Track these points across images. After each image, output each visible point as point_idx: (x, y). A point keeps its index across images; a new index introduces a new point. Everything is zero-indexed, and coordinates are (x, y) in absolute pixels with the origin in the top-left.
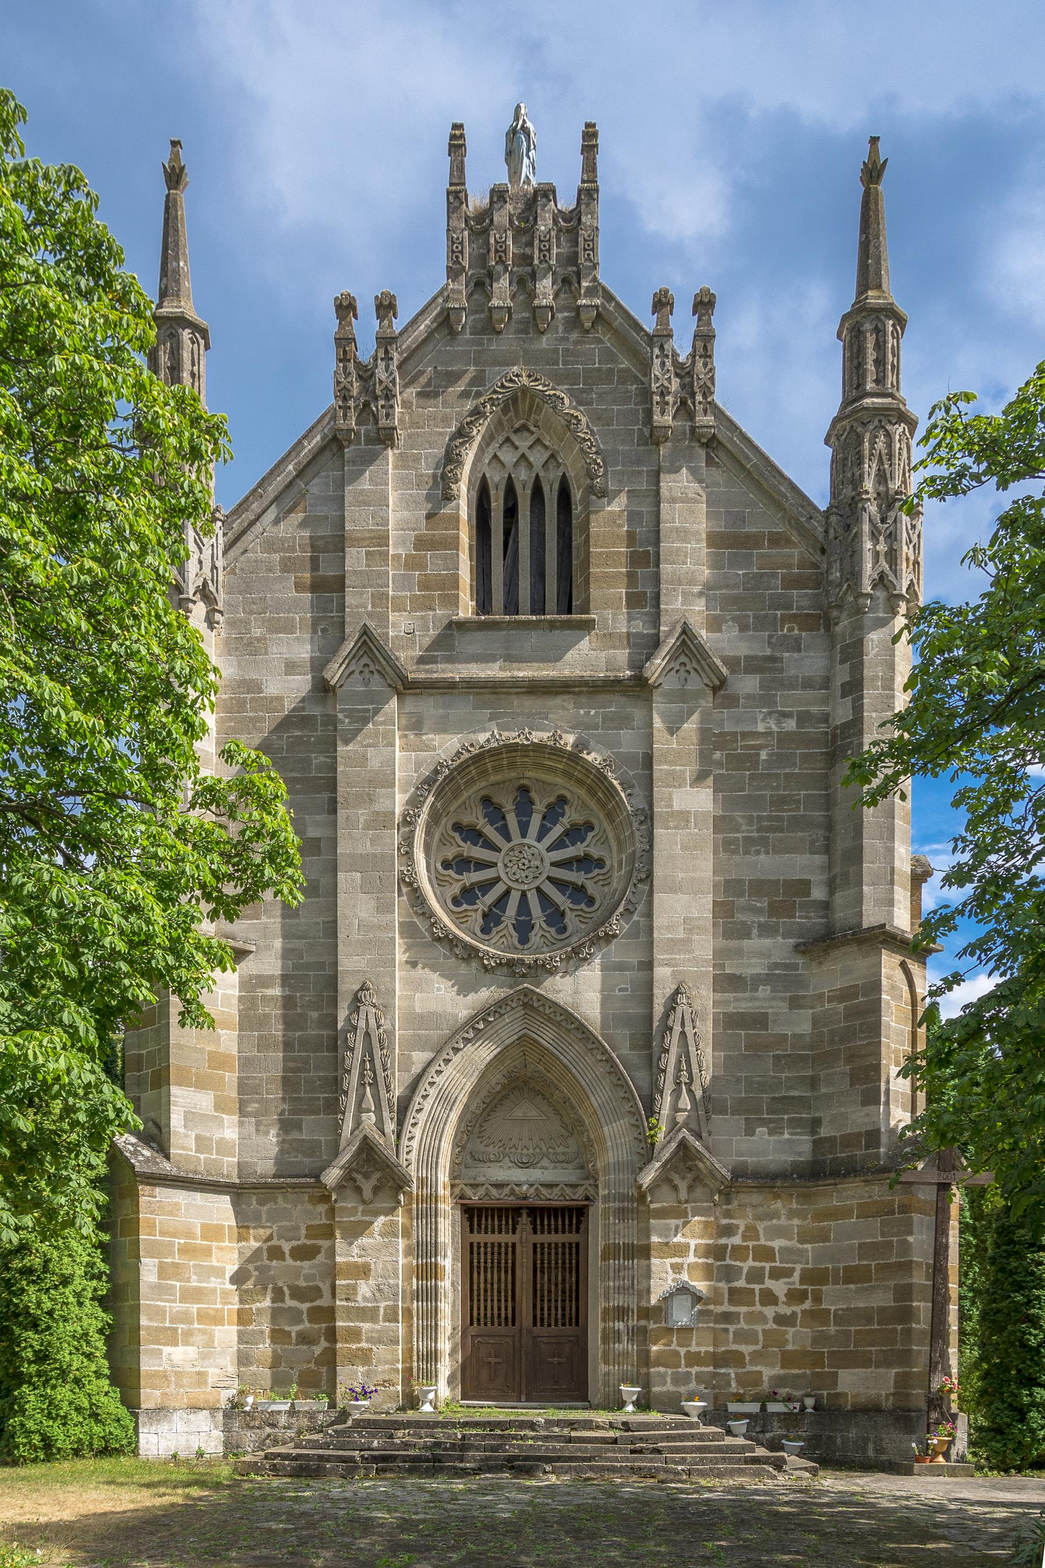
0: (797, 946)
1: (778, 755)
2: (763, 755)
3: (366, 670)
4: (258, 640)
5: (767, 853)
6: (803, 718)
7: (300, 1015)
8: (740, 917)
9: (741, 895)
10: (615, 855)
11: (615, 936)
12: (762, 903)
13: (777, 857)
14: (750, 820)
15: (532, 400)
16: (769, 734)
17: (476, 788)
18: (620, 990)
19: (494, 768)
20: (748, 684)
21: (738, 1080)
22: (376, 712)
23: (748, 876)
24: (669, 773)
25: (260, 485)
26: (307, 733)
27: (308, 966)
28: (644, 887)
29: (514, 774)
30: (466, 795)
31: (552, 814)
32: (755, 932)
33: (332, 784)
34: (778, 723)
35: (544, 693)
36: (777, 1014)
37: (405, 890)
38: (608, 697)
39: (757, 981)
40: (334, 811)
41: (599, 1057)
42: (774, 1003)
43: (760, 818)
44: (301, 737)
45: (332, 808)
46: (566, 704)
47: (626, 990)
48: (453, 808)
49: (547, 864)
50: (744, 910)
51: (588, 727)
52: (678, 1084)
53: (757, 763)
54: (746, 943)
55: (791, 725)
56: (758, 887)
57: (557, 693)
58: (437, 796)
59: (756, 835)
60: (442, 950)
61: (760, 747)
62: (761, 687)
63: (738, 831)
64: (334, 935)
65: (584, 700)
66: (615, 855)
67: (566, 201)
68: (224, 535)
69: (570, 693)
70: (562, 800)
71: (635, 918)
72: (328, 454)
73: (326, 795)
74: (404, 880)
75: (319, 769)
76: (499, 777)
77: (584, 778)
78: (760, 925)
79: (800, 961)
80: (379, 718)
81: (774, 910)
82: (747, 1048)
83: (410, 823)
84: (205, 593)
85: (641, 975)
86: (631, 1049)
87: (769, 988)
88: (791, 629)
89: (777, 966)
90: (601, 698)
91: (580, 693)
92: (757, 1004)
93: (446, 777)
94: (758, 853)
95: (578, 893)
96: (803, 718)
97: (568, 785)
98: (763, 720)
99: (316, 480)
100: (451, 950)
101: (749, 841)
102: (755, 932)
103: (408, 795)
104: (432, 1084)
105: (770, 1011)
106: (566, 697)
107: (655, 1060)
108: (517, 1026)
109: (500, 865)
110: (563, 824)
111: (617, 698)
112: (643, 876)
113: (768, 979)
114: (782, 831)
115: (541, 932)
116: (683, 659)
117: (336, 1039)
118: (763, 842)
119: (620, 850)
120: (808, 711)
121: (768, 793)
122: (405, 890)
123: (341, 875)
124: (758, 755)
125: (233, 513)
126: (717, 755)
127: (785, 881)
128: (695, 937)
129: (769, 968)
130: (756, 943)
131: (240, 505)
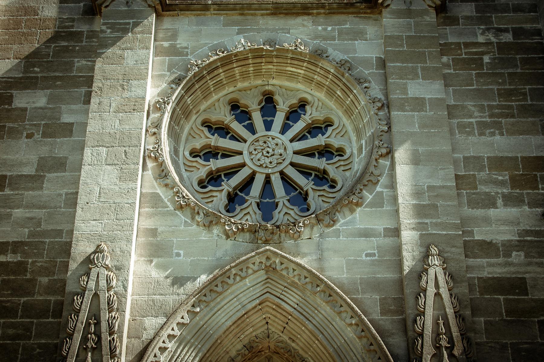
1: (501, 59)
2: (486, 59)
5: (502, 134)
7: (28, 281)
8: (483, 188)
9: (482, 169)
10: (354, 144)
11: (358, 205)
12: (505, 176)
13: (512, 138)
14: (482, 108)
16: (488, 44)
17: (225, 92)
18: (367, 255)
19: (242, 74)
21: (504, 347)
23: (486, 153)
24: (401, 68)
26: (72, 44)
27: (45, 234)
28: (385, 163)
29: (259, 82)
30: (215, 97)
31: (293, 115)
33: (89, 81)
34: (496, 36)
35: (287, 14)
36: (534, 279)
37: (150, 164)
38: (342, 17)
39: (508, 248)
40: (87, 101)
41: (348, 321)
42: (529, 268)
43: (490, 107)
44: (67, 47)
46: (305, 23)
47: (374, 255)
48: (203, 107)
49: (290, 151)
50: (485, 182)
51: (325, 39)
52: (438, 348)
53: (482, 65)
54: (492, 212)
55: (508, 37)
56: (498, 163)
57: (298, 14)
58: (188, 89)
59: (488, 120)
60: (182, 217)
61: (483, 53)
62: (477, 12)
63: (471, 117)
65: (321, 19)
66: (354, 144)
69: (309, 14)
70: (303, 105)
71: (378, 189)
74: (150, 157)
75: (80, 69)
76: (246, 84)
77: (324, 82)
81: (515, 182)
82: (508, 313)
83: (160, 109)
85: (389, 241)
86: (382, 314)
87: (522, 254)
89: (528, 232)
90: (336, 18)
91: (318, 14)
92: (512, 269)
93: (195, 75)
94: (493, 134)
95: (322, 178)
96: (517, 33)
97: (309, 90)
98: (482, 34)
100: (193, 218)
101: (482, 126)
102: (500, 202)
103: (160, 89)
104: (163, 350)
105: (527, 276)
106: (306, 18)
107: (409, 323)
108: (258, 290)
109: (245, 153)
110: (304, 120)
112: (384, 151)
113: (520, 245)
114: (513, 116)
115: (285, 210)
117: (62, 303)
118: (497, 126)
119: (359, 137)
120: (521, 28)
121: (495, 87)
122: (150, 164)
123: (88, 152)
124: (482, 59)
126: (445, 59)
127: (523, 158)
128: (440, 203)
129: (520, 235)
130: (501, 211)
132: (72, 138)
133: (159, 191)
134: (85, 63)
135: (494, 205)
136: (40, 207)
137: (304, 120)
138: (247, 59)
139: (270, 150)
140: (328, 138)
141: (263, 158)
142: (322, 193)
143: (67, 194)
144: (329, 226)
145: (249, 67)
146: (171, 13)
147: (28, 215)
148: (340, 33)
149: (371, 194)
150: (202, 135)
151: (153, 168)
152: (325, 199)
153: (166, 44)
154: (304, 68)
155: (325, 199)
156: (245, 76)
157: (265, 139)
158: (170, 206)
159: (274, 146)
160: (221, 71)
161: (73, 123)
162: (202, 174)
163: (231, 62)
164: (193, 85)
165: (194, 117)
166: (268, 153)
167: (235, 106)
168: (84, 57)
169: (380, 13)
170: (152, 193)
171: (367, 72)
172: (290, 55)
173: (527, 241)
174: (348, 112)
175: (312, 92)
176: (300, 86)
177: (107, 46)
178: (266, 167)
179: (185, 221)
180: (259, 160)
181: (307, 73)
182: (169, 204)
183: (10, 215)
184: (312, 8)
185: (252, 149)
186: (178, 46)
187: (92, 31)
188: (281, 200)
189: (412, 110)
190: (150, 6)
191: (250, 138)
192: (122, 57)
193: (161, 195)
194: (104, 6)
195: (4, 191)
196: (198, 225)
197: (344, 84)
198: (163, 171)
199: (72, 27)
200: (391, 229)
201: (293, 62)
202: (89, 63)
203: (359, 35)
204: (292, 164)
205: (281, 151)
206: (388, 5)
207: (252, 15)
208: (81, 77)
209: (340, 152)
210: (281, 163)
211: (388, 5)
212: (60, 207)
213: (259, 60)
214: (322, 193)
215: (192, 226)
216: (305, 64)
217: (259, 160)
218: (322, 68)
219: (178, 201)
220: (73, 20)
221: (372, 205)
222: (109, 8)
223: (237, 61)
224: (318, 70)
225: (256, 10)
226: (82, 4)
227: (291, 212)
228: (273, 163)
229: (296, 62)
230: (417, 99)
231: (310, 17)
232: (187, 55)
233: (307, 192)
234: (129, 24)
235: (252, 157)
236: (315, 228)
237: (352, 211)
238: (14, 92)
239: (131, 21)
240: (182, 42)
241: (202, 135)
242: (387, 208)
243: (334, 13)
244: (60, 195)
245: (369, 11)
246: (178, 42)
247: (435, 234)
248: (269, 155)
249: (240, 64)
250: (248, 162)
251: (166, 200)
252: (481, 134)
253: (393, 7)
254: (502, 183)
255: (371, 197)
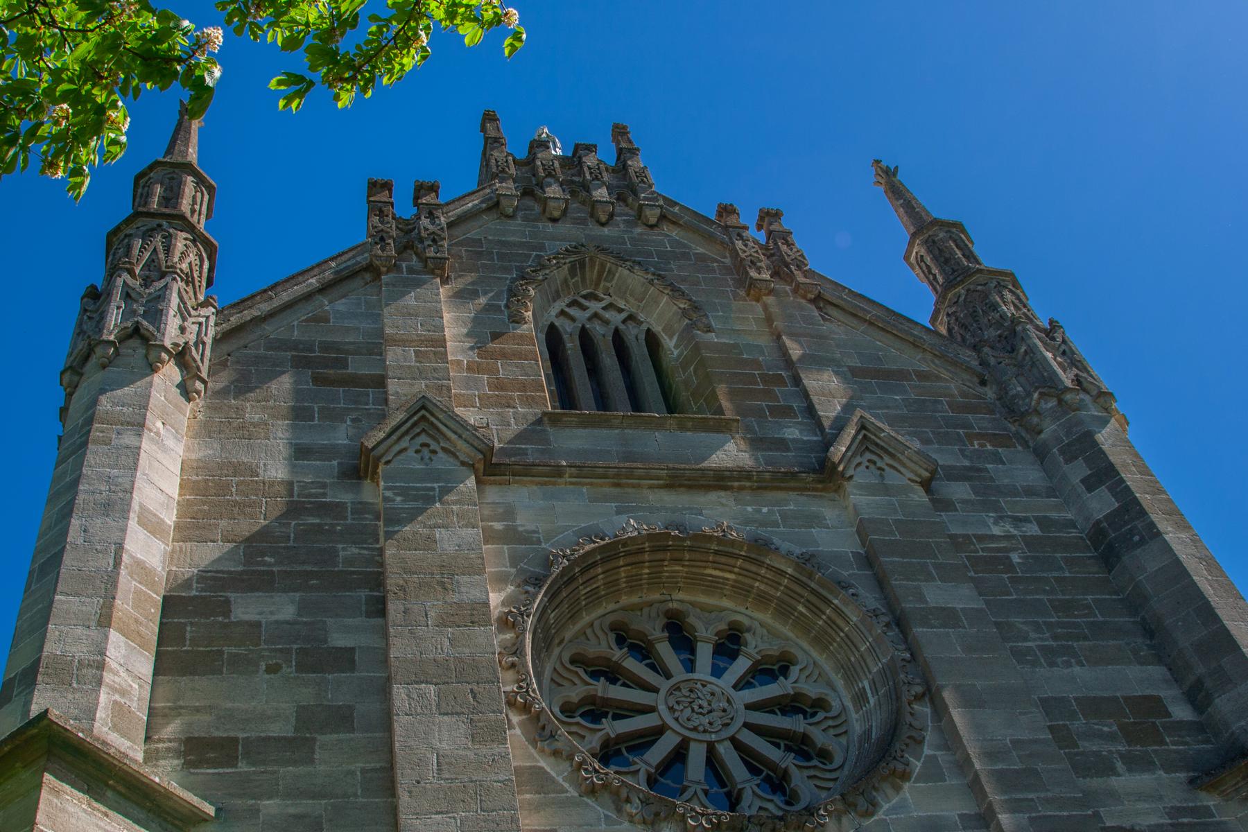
0: (1192, 781)
3: (425, 451)
4: (255, 425)
6: (1043, 522)
15: (603, 266)
20: (960, 491)
22: (446, 491)
25: (272, 288)
26: (329, 521)
32: (1119, 766)
35: (690, 487)
38: (780, 495)
44: (319, 525)
45: (379, 608)
54: (1114, 782)
55: (1033, 530)
57: (708, 488)
58: (552, 595)
60: (598, 809)
63: (1026, 639)
64: (391, 788)
67: (607, 154)
68: (216, 324)
69: (725, 488)
71: (927, 751)
72: (358, 282)
73: (363, 594)
78: (1122, 756)
79: (1210, 800)
80: (451, 497)
83: (514, 625)
84: (181, 356)
88: (981, 445)
91: (741, 488)
93: (562, 574)
94: (1068, 665)
96: (1043, 522)
99: (344, 300)
100: (619, 810)
101: (1049, 652)
102: (1119, 766)
106: (722, 493)
111: (792, 495)
114: (1085, 638)
116: (868, 456)
125: (233, 306)
131: (243, 301)
132: (356, 674)
133: (542, 764)
134: (357, 551)
135: (1112, 771)
136: (314, 796)
137: (749, 656)
138: (641, 551)
139: (705, 704)
140: (795, 682)
141: (695, 716)
142: (812, 772)
143: (363, 771)
144: (868, 814)
145: (643, 568)
146: (497, 478)
147: (292, 810)
148: (784, 516)
149: (918, 760)
150: (576, 680)
151: (521, 724)
152: (819, 783)
153: (498, 526)
154: (736, 570)
155: (819, 783)
156: (634, 584)
157: (691, 685)
158: (570, 789)
159: (709, 697)
160: (600, 570)
161: (353, 649)
162: (594, 744)
163: (616, 557)
164: (559, 590)
165: (557, 651)
166: (700, 707)
167: (622, 635)
168: (354, 543)
169: (838, 489)
170: (531, 767)
171: (846, 574)
172: (714, 547)
173: (1183, 824)
174: (821, 641)
175: (748, 612)
176: (726, 603)
177: (401, 522)
178: (705, 731)
179: (606, 816)
180: (689, 720)
181: (740, 578)
182: (566, 785)
183: (255, 812)
184: (732, 479)
185: (672, 702)
186: (520, 529)
187: (361, 503)
188: (747, 785)
189: (944, 626)
190: (463, 464)
191: (665, 685)
192: (431, 539)
193: (548, 770)
194: (383, 461)
195: (235, 766)
196: (631, 821)
197: (813, 591)
198: (543, 728)
199: (324, 495)
200: (970, 815)
201: (718, 558)
202: (366, 552)
203: (814, 520)
204: (746, 725)
205: (724, 704)
206: (851, 477)
207: (633, 486)
208: (354, 573)
209: (820, 704)
210: (728, 724)
211: (851, 477)
212: (356, 795)
213: (659, 556)
214: (812, 772)
215: (621, 824)
216: (739, 562)
217: (689, 720)
218: (770, 568)
219: (587, 779)
220: (324, 486)
221: (925, 777)
222: (392, 465)
223: (628, 554)
224: (763, 571)
225: (640, 478)
226: (335, 463)
227: (770, 806)
228: (715, 725)
229: (723, 559)
230: (943, 609)
231: (729, 493)
232: (539, 542)
233: (786, 771)
234: (433, 489)
235: (677, 714)
236: (844, 820)
237: (898, 789)
238: (232, 596)
239: (436, 485)
240: (524, 522)
241: (576, 680)
242: (953, 781)
243: (765, 488)
244: (352, 773)
245: (820, 486)
246: (518, 522)
247: (1050, 816)
248: (705, 711)
249: (629, 560)
250: (670, 722)
251: (560, 780)
252: (1052, 664)
253: (858, 479)
254: (1111, 737)
255: (919, 764)
